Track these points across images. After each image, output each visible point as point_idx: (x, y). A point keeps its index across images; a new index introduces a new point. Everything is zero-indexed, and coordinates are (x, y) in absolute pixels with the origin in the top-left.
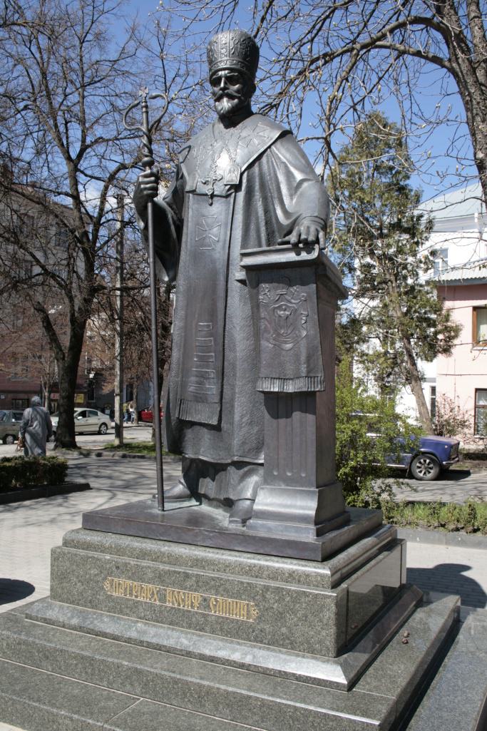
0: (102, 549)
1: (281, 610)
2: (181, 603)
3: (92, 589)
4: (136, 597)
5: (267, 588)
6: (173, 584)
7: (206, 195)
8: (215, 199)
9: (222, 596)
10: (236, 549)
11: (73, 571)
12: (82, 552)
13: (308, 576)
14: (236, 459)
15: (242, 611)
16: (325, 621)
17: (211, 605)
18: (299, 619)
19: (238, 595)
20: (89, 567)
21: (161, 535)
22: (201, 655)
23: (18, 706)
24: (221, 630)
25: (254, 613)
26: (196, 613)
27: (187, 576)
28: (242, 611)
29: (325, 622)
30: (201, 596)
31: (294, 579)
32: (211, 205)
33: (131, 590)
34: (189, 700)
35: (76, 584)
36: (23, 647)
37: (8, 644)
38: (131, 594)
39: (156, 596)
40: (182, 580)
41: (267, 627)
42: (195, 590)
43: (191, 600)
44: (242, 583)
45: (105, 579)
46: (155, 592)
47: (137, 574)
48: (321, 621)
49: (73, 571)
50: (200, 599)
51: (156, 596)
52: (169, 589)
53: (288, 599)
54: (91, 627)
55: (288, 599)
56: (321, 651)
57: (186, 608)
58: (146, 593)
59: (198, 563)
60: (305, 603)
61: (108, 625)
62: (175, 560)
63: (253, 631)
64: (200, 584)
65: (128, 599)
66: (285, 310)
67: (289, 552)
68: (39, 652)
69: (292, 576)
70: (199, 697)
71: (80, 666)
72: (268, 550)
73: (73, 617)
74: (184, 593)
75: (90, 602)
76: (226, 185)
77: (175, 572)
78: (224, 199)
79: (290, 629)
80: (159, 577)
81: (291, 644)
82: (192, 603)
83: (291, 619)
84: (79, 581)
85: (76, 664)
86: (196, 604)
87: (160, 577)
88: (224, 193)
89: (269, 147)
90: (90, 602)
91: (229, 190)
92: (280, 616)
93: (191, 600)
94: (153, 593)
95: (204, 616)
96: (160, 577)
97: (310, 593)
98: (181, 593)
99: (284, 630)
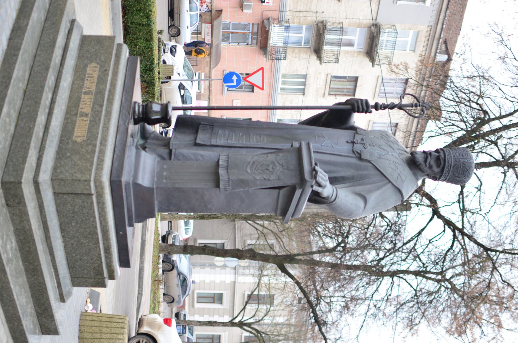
1: (81, 153)
2: (84, 103)
4: (87, 80)
5: (95, 146)
6: (96, 98)
7: (354, 139)
8: (351, 145)
9: (89, 123)
10: (118, 136)
11: (102, 47)
12: (114, 52)
13: (102, 169)
16: (74, 175)
17: (83, 118)
20: (105, 55)
21: (126, 98)
24: (67, 123)
25: (79, 140)
26: (78, 110)
27: (102, 106)
29: (74, 175)
30: (89, 113)
31: (100, 162)
32: (347, 142)
33: (91, 77)
34: (31, 93)
35: (94, 48)
36: (59, 12)
38: (89, 77)
39: (88, 90)
40: (98, 104)
41: (70, 146)
42: (92, 110)
45: (98, 63)
46: (90, 89)
47: (101, 80)
48: (75, 173)
49: (102, 47)
50: (87, 112)
52: (93, 97)
53: (88, 156)
55: (88, 156)
56: (56, 173)
57: (81, 105)
58: (90, 85)
60: (86, 165)
62: (111, 101)
63: (67, 139)
64: (97, 113)
65: (85, 75)
66: (273, 168)
67: (116, 164)
69: (101, 161)
70: (33, 98)
71: (49, 40)
72: (117, 152)
74: (90, 104)
75: (83, 56)
76: (361, 151)
78: (351, 150)
79: (70, 157)
80: (100, 92)
81: (60, 158)
82: (84, 108)
83: (76, 158)
84: (96, 50)
85: (50, 38)
86: (83, 110)
87: (100, 92)
88: (355, 150)
89: (390, 181)
90: (83, 56)
91: (358, 153)
95: (76, 114)
96: (100, 92)
97: (92, 168)
98: (90, 103)
99: (68, 154)
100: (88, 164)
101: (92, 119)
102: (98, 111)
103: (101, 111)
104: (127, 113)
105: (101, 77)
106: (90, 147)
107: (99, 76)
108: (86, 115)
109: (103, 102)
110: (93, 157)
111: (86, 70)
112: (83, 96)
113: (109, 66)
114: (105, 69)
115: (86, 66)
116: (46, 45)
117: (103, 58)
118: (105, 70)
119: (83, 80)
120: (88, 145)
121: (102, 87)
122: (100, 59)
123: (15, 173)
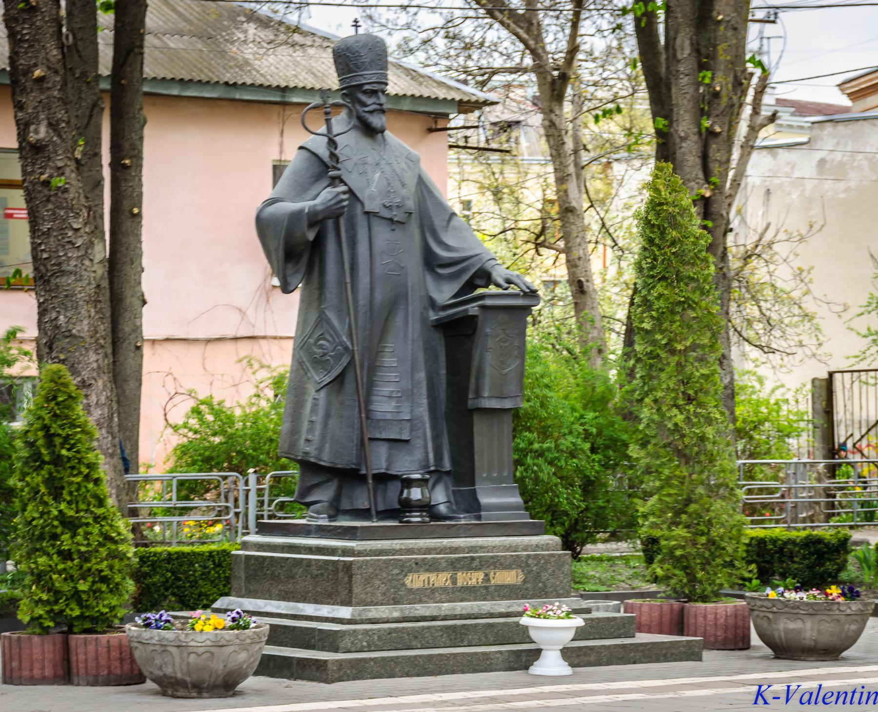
0: (394, 552)
3: (394, 587)
5: (529, 556)
6: (461, 568)
14: (432, 468)
15: (510, 577)
18: (550, 575)
19: (509, 567)
22: (500, 613)
23: (458, 658)
24: (499, 596)
25: (521, 577)
27: (473, 559)
28: (510, 577)
36: (394, 635)
37: (379, 637)
38: (429, 584)
39: (449, 581)
40: (469, 564)
42: (480, 569)
43: (476, 578)
44: (512, 556)
45: (406, 576)
47: (433, 567)
49: (377, 575)
51: (449, 581)
52: (459, 574)
54: (412, 615)
55: (542, 561)
58: (441, 579)
59: (473, 549)
61: (420, 609)
67: (526, 531)
68: (408, 634)
71: (445, 635)
73: (391, 612)
75: (393, 599)
77: (464, 558)
83: (545, 576)
86: (480, 580)
92: (538, 575)
93: (476, 578)
94: (446, 580)
95: (486, 588)
99: (540, 585)
100: (553, 559)
101: (492, 567)
102: (481, 562)
103: (481, 557)
104: (455, 528)
105: (427, 567)
106: (530, 561)
107: (427, 570)
108: (486, 575)
109: (466, 558)
110: (543, 556)
111: (418, 589)
112: (459, 584)
113: (411, 560)
114: (414, 565)
115: (410, 590)
116: (453, 637)
117: (396, 571)
118: (417, 564)
119: (433, 590)
120: (528, 565)
121: (444, 564)
122: (397, 574)
123: (627, 625)
